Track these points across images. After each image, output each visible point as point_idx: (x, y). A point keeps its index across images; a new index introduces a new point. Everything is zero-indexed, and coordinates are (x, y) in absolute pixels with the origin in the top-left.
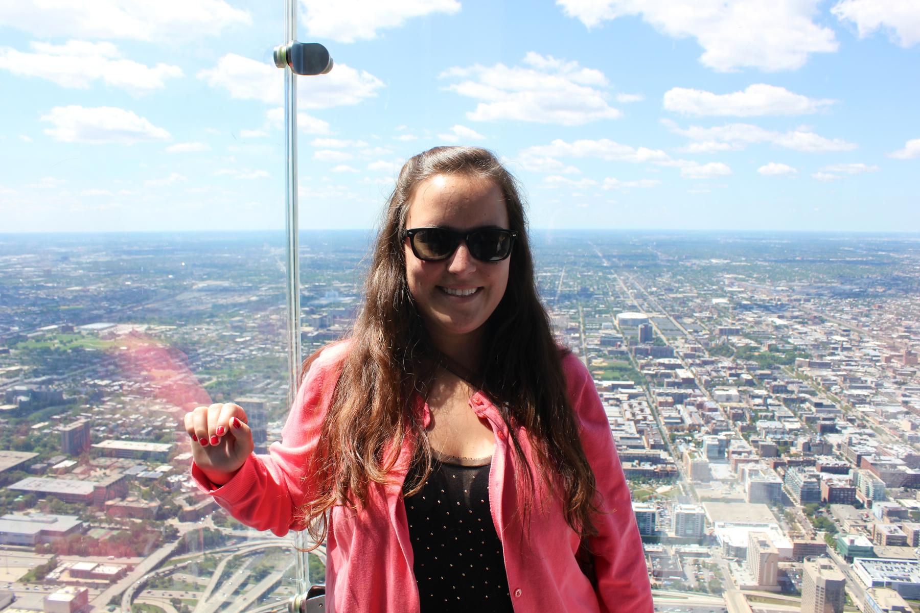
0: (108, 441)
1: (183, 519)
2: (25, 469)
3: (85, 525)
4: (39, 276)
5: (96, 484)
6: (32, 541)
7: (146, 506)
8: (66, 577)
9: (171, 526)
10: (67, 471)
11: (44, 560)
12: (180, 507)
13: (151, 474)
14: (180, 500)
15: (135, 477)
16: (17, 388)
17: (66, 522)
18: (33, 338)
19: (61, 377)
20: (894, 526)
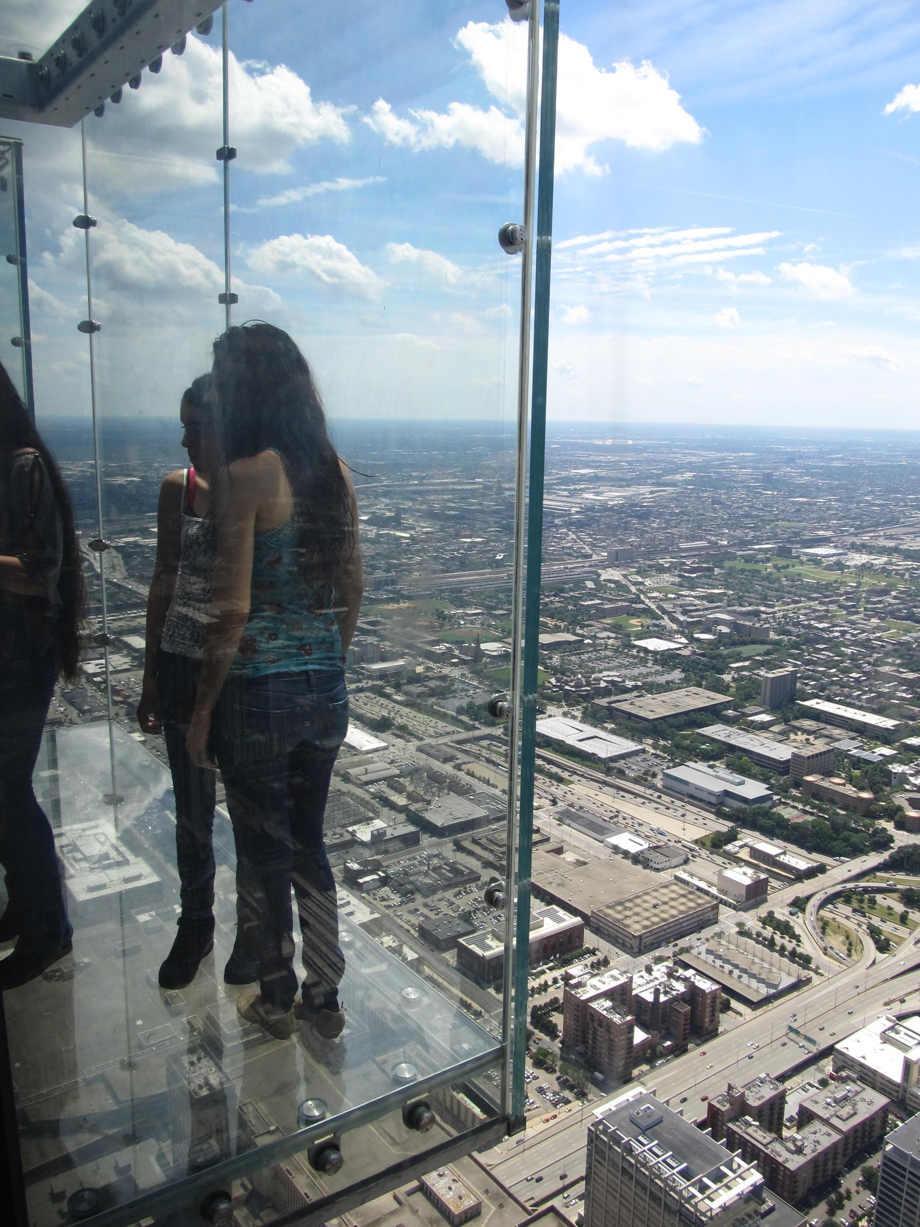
0: (817, 700)
1: (900, 826)
2: (714, 714)
3: (775, 798)
4: (757, 480)
5: (795, 750)
6: (713, 800)
7: (855, 795)
8: (744, 854)
9: (884, 830)
10: (764, 727)
11: (724, 826)
12: (900, 809)
13: (865, 755)
14: (900, 799)
15: (845, 754)
16: (719, 615)
17: (753, 789)
18: (742, 556)
19: (770, 610)
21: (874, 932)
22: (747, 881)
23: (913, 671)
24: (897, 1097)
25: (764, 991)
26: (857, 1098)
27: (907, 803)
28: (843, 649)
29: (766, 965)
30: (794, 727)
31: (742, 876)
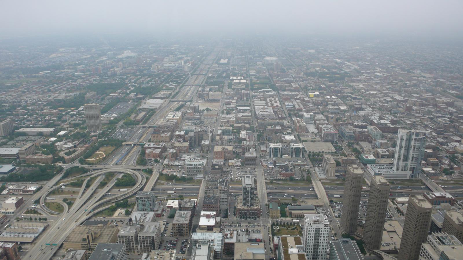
1: (64, 162)
3: (17, 168)
12: (63, 157)
14: (62, 154)
20: (385, 150)
21: (65, 200)
22: (15, 202)
23: (55, 109)
24: (88, 248)
25: (33, 236)
26: (76, 255)
27: (64, 155)
28: (28, 107)
29: (31, 228)
30: (17, 140)
31: (12, 201)
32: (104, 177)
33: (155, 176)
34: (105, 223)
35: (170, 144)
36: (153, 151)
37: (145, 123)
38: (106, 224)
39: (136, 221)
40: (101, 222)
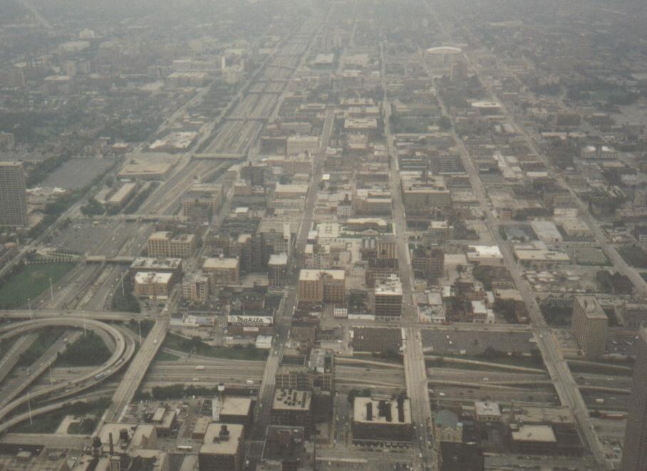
32: (36, 336)
33: (154, 339)
34: (35, 450)
35: (193, 261)
36: (152, 278)
37: (133, 210)
38: (38, 454)
39: (111, 445)
40: (26, 448)
